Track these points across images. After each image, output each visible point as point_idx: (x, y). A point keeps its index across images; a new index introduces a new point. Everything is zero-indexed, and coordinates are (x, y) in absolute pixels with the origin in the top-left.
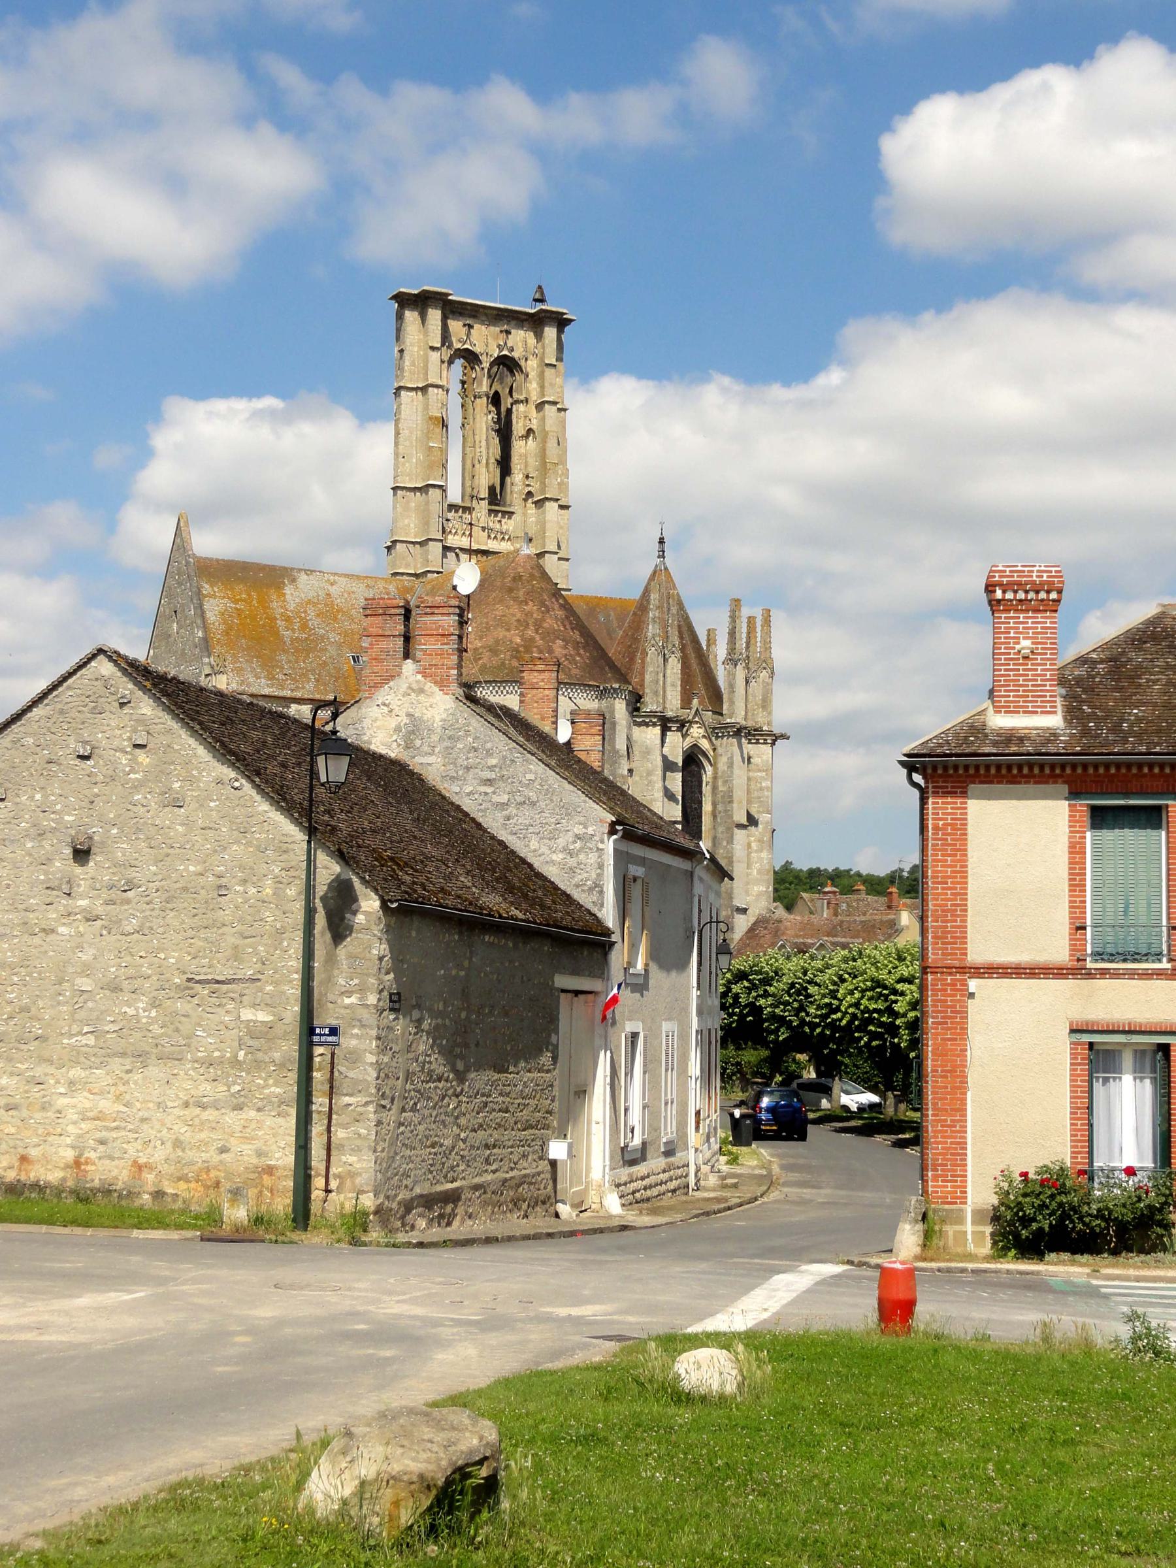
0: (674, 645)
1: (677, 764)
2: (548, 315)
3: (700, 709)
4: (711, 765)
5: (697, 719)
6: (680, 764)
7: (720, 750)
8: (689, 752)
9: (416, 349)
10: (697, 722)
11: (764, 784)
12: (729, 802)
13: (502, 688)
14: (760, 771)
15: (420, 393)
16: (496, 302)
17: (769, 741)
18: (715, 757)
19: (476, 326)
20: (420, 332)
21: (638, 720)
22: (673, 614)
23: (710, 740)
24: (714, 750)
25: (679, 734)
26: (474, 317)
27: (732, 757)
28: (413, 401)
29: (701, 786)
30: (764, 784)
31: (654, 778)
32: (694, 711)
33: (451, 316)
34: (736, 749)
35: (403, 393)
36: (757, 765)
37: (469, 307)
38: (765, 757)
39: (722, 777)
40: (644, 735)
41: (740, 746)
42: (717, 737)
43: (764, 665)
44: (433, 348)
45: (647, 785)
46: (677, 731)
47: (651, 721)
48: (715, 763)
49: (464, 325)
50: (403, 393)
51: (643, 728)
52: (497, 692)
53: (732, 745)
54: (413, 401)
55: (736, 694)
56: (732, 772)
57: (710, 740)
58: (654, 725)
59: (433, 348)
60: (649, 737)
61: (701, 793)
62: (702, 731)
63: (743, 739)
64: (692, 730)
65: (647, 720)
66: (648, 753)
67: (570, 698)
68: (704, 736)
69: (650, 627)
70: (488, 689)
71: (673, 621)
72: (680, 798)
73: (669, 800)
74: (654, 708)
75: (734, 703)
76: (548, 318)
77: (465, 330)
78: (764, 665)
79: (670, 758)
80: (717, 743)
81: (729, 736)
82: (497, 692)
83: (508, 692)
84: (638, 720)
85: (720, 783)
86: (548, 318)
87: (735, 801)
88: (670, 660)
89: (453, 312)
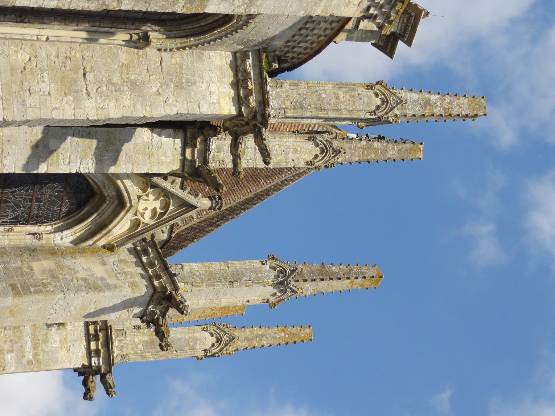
0: (337, 152)
1: (114, 161)
2: (412, 21)
3: (193, 213)
4: (78, 242)
5: (171, 208)
6: (112, 170)
7: (111, 258)
8: (109, 193)
10: (166, 207)
11: (9, 357)
12: (14, 287)
14: (35, 346)
17: (94, 360)
18: (94, 251)
21: (249, 62)
22: (385, 151)
23: (129, 238)
24: (110, 248)
25: (176, 166)
27: (108, 287)
29: (27, 222)
30: (9, 357)
31: (127, 100)
32: (191, 199)
34: (128, 293)
36: (45, 341)
38: (62, 354)
39: (61, 267)
40: (215, 76)
41: (127, 304)
42: (135, 252)
43: (225, 338)
45: (110, 82)
46: (184, 160)
47: (250, 92)
48: (83, 251)
51: (229, 77)
53: (133, 285)
55: (228, 289)
56: (78, 290)
57: (129, 238)
58: (239, 101)
60: (213, 88)
61: (15, 222)
62: (147, 219)
63: (137, 310)
64: (151, 197)
65: (250, 85)
66: (179, 86)
68: (136, 224)
69: (414, 96)
71: (377, 150)
72: (43, 169)
73: (36, 147)
74: (273, 103)
75: (212, 284)
76: (408, 19)
78: (225, 338)
79: (127, 148)
80: (124, 253)
81: (150, 279)
84: (249, 62)
85: (48, 264)
86: (408, 19)
87: (18, 301)
88: (310, 145)
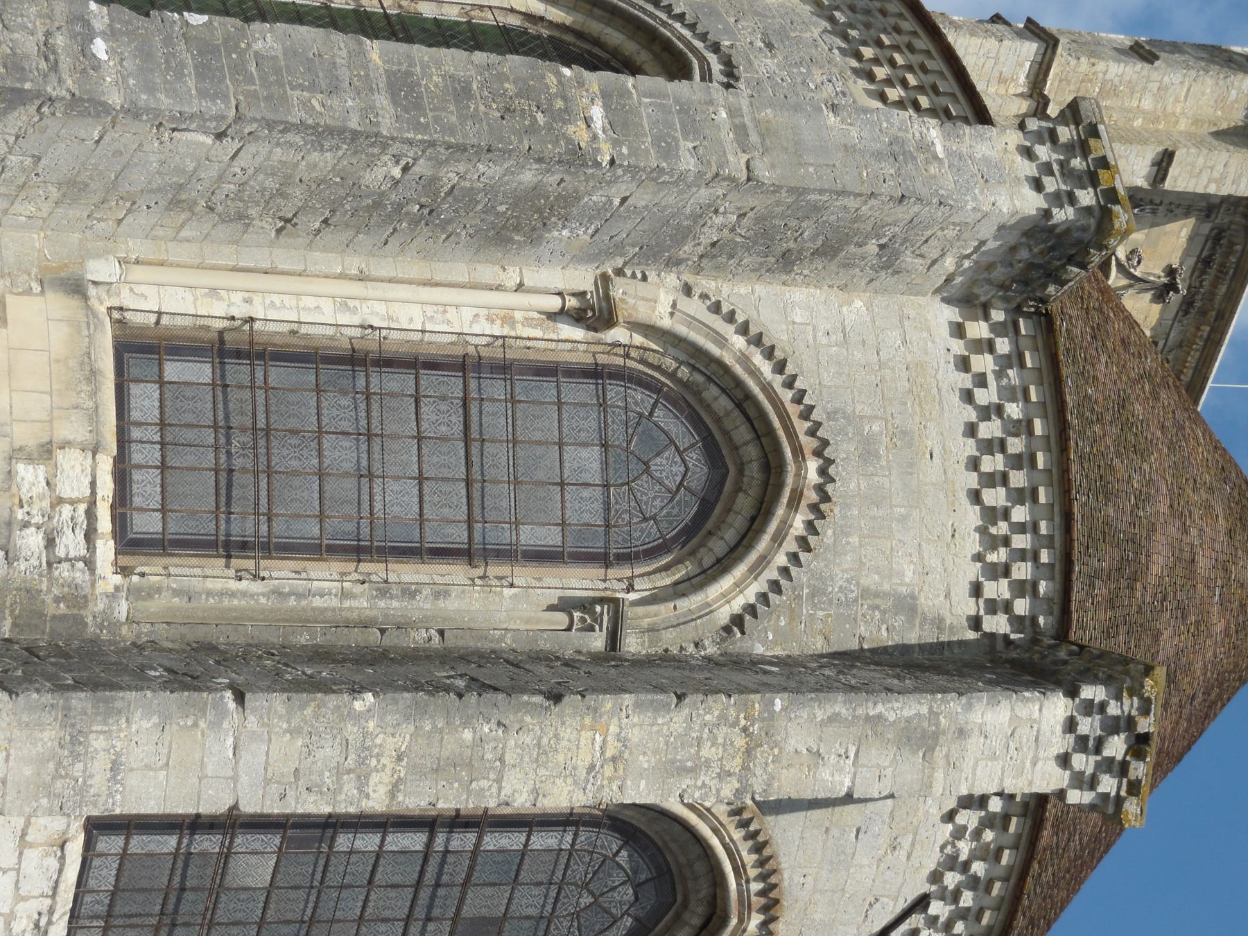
9: (1147, 104)
13: (1018, 479)
15: (1024, 106)
16: (1212, 383)
19: (1157, 308)
20: (1197, 122)
26: (1187, 304)
28: (1002, 80)
33: (1206, 228)
35: (1030, 49)
37: (1223, 289)
44: (1164, 161)
49: (1171, 272)
50: (1030, 49)
52: (989, 446)
54: (1002, 80)
59: (1164, 161)
67: (922, 903)
70: (1010, 393)
77: (1153, 269)
82: (989, 446)
83: (992, 515)
89: (1217, 237)
